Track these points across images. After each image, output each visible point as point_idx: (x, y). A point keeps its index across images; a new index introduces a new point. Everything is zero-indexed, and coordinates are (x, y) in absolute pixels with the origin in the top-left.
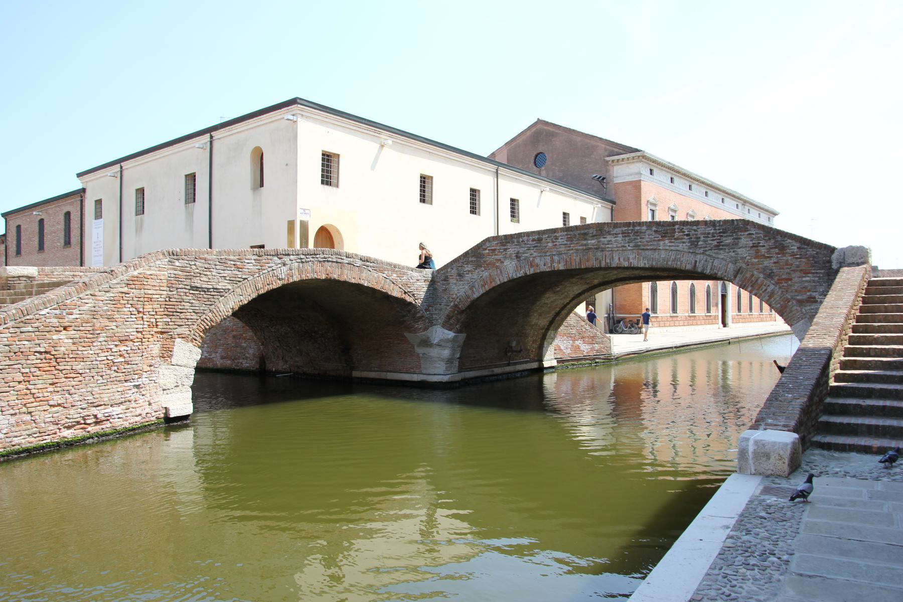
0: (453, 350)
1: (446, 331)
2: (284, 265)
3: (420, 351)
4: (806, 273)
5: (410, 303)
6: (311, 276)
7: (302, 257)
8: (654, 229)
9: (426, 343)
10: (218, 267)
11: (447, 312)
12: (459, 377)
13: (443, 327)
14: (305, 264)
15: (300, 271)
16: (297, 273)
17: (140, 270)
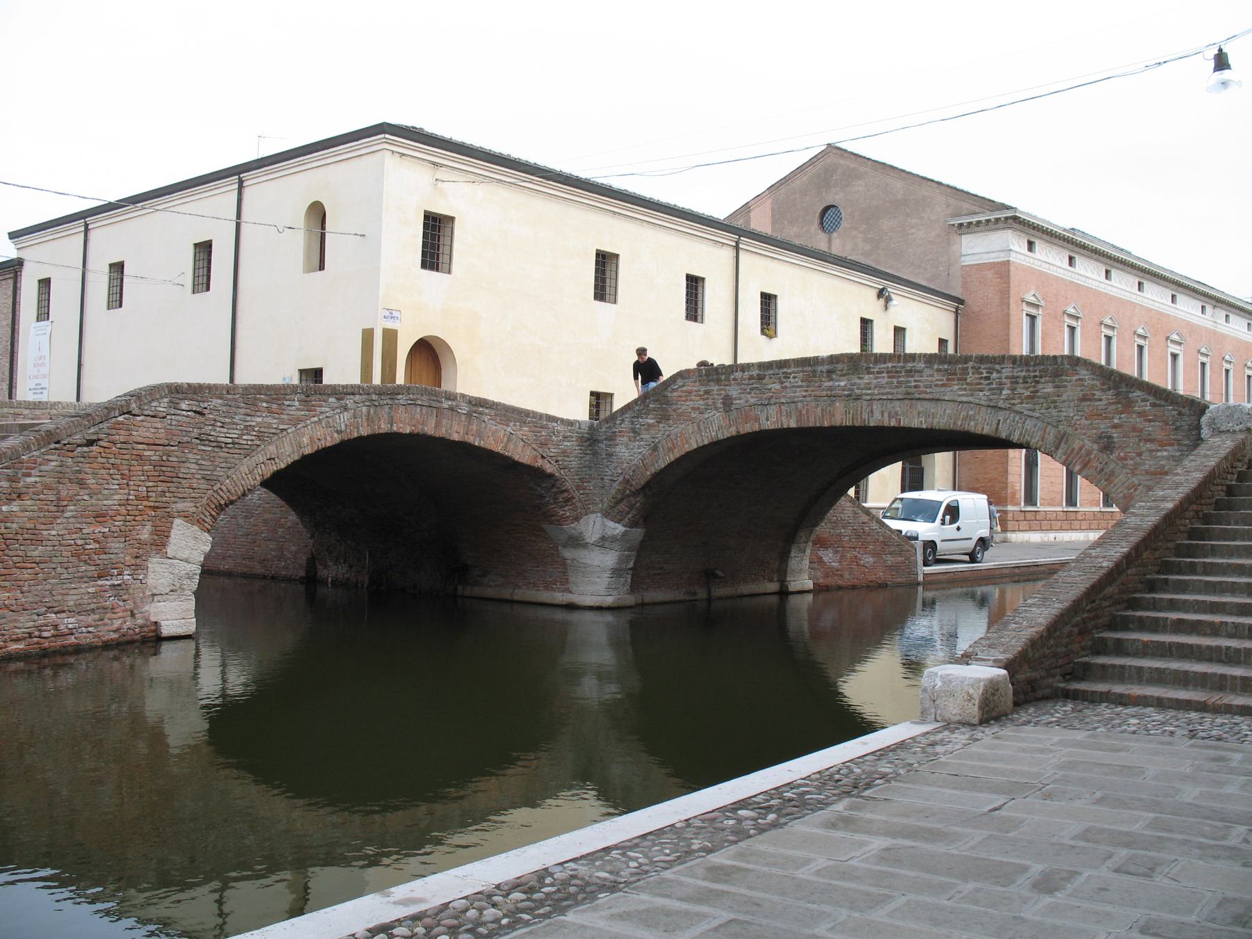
1: (611, 524)
2: (346, 409)
3: (568, 553)
4: (1163, 445)
5: (551, 476)
6: (384, 428)
7: (374, 397)
8: (936, 367)
9: (577, 542)
11: (613, 492)
12: (630, 600)
13: (606, 514)
14: (379, 409)
15: (369, 418)
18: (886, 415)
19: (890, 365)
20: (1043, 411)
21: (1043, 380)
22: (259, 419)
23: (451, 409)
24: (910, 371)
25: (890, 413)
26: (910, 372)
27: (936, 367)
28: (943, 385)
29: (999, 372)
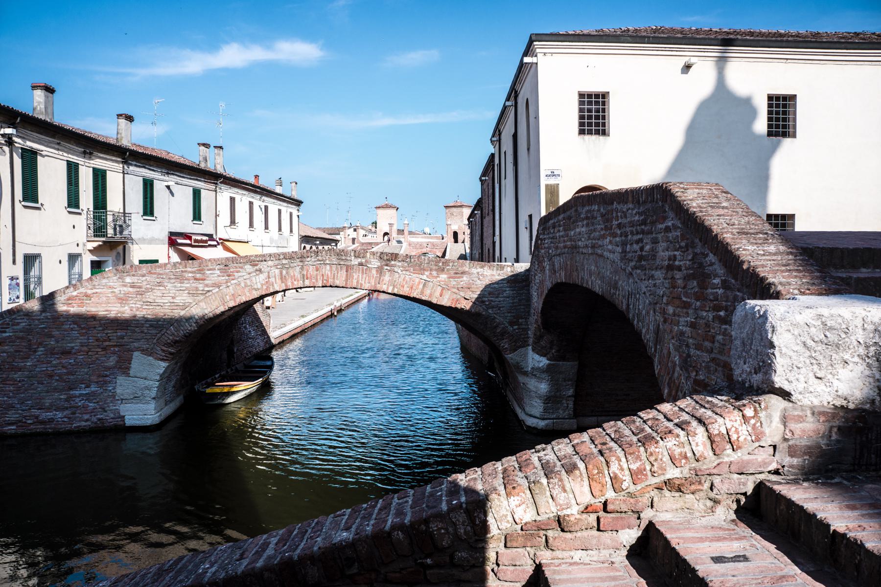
0: (555, 385)
1: (537, 357)
7: (284, 262)
10: (173, 281)
14: (291, 271)
16: (279, 281)
17: (82, 290)
22: (188, 285)
23: (361, 264)
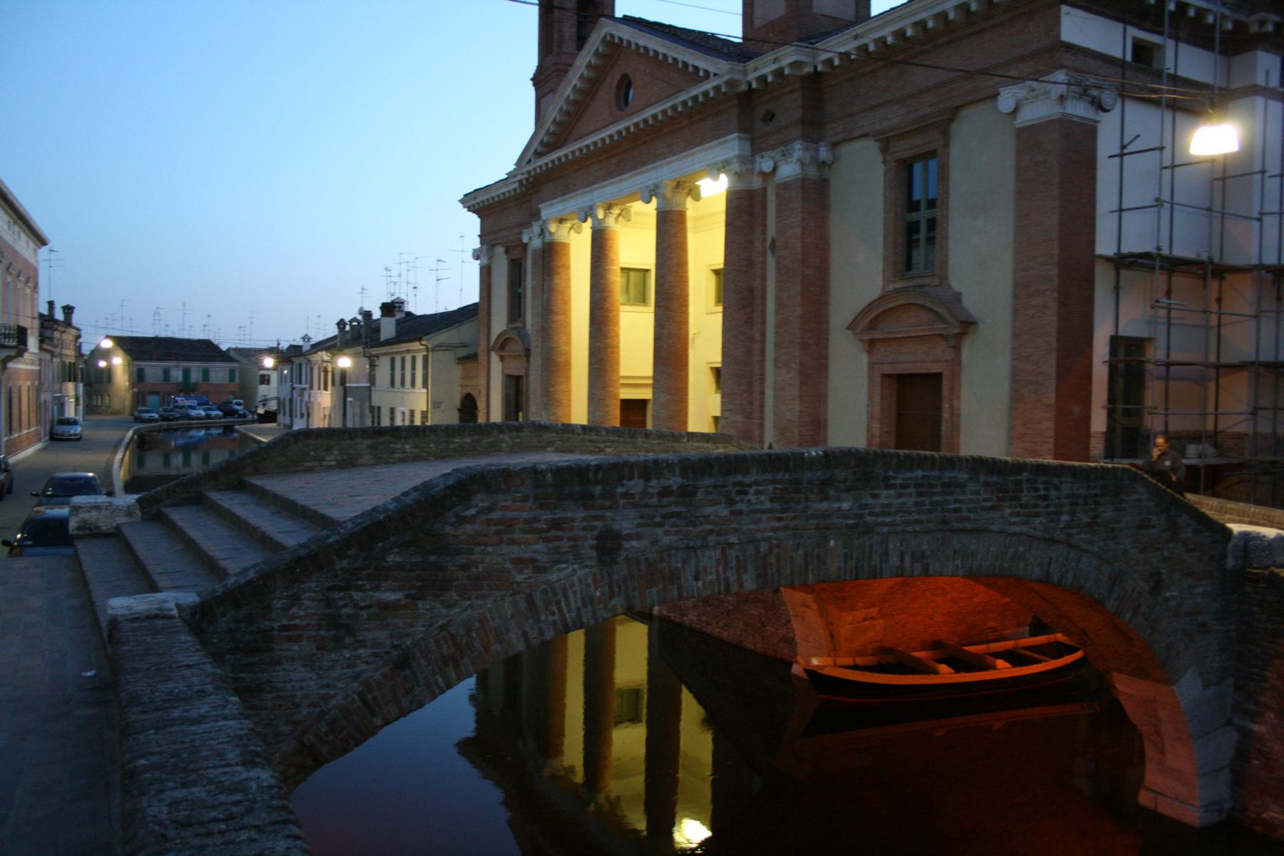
18: (907, 559)
19: (919, 473)
20: (1102, 544)
21: (1102, 500)
24: (948, 485)
25: (913, 555)
26: (949, 487)
27: (982, 478)
28: (992, 508)
29: (1057, 488)
